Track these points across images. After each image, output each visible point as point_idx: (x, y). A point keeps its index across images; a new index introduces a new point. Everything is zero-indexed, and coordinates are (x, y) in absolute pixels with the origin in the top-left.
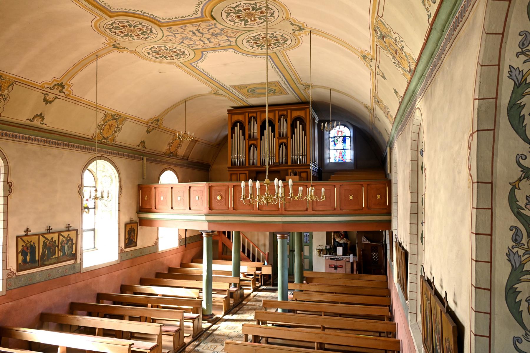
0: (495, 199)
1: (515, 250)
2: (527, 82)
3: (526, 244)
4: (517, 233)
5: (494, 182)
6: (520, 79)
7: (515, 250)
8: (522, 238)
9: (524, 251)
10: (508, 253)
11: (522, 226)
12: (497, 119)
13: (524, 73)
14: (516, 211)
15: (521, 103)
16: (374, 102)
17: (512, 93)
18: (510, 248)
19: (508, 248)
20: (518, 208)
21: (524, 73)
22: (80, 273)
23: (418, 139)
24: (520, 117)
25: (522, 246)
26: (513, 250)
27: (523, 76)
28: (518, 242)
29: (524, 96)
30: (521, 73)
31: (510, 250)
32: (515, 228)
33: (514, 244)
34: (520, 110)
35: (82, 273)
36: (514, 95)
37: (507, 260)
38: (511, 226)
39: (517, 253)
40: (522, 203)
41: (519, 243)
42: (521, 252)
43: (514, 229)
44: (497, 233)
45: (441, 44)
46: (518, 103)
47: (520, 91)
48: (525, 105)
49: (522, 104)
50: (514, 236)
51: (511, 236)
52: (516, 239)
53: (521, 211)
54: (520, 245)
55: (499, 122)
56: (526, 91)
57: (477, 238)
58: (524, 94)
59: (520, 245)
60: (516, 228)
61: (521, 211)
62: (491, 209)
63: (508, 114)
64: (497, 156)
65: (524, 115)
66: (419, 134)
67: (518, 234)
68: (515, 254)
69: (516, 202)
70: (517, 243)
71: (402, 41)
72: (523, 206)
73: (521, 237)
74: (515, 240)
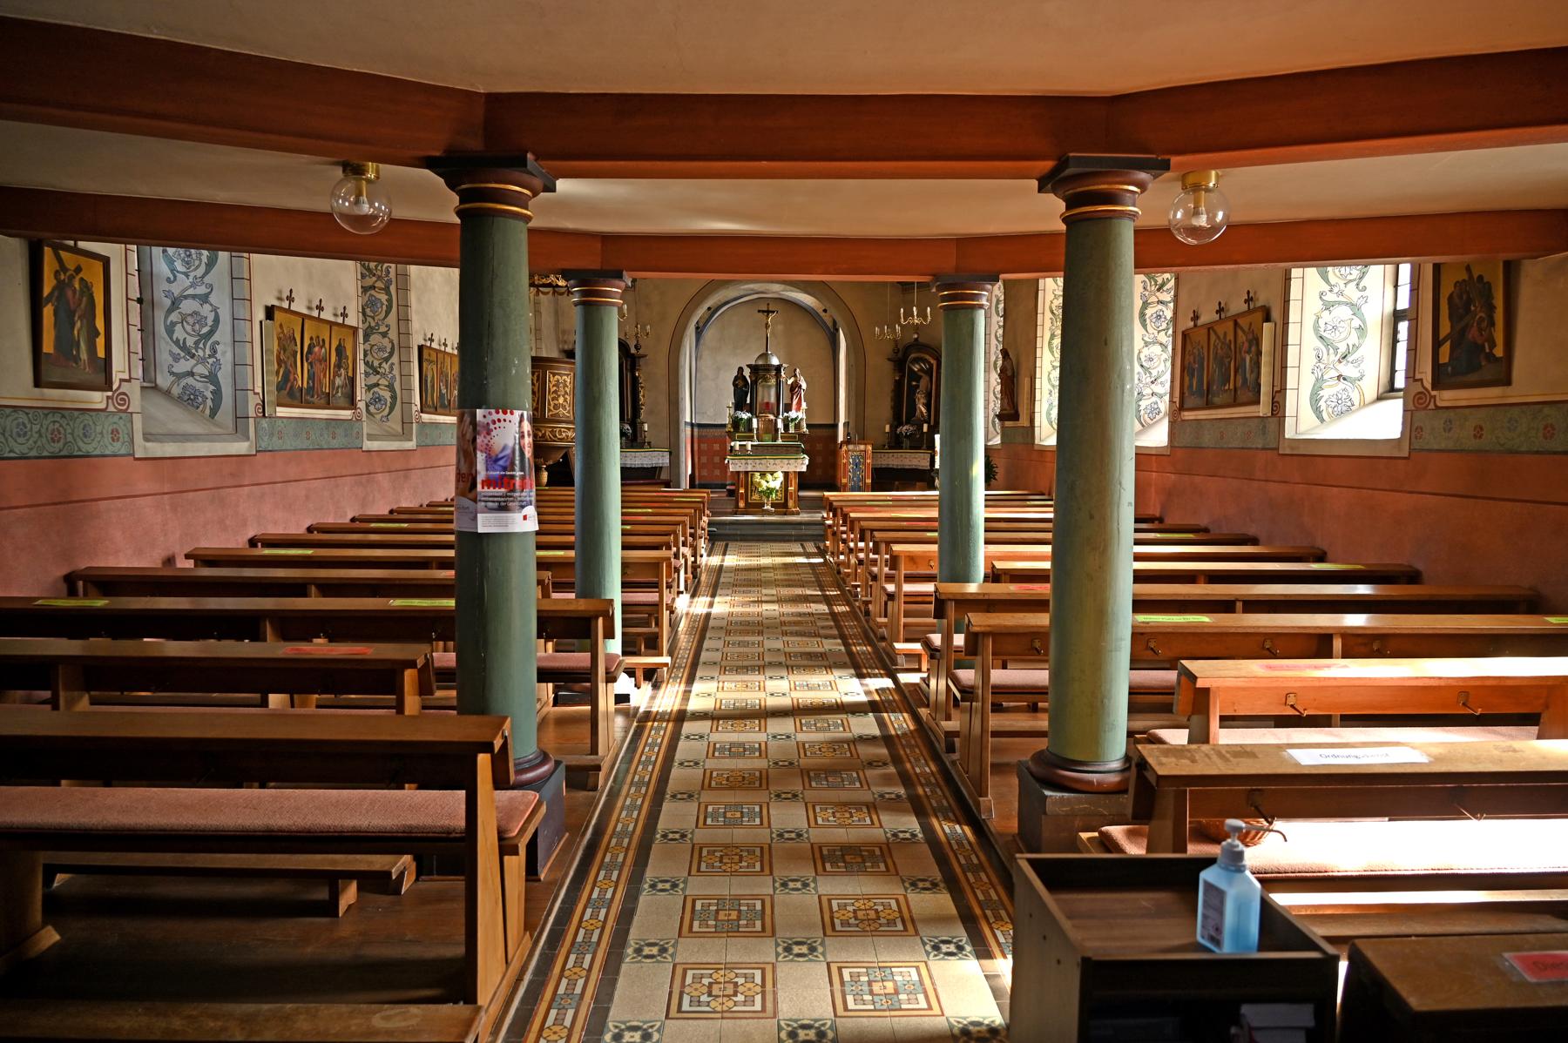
22: (1275, 452)
35: (1283, 455)
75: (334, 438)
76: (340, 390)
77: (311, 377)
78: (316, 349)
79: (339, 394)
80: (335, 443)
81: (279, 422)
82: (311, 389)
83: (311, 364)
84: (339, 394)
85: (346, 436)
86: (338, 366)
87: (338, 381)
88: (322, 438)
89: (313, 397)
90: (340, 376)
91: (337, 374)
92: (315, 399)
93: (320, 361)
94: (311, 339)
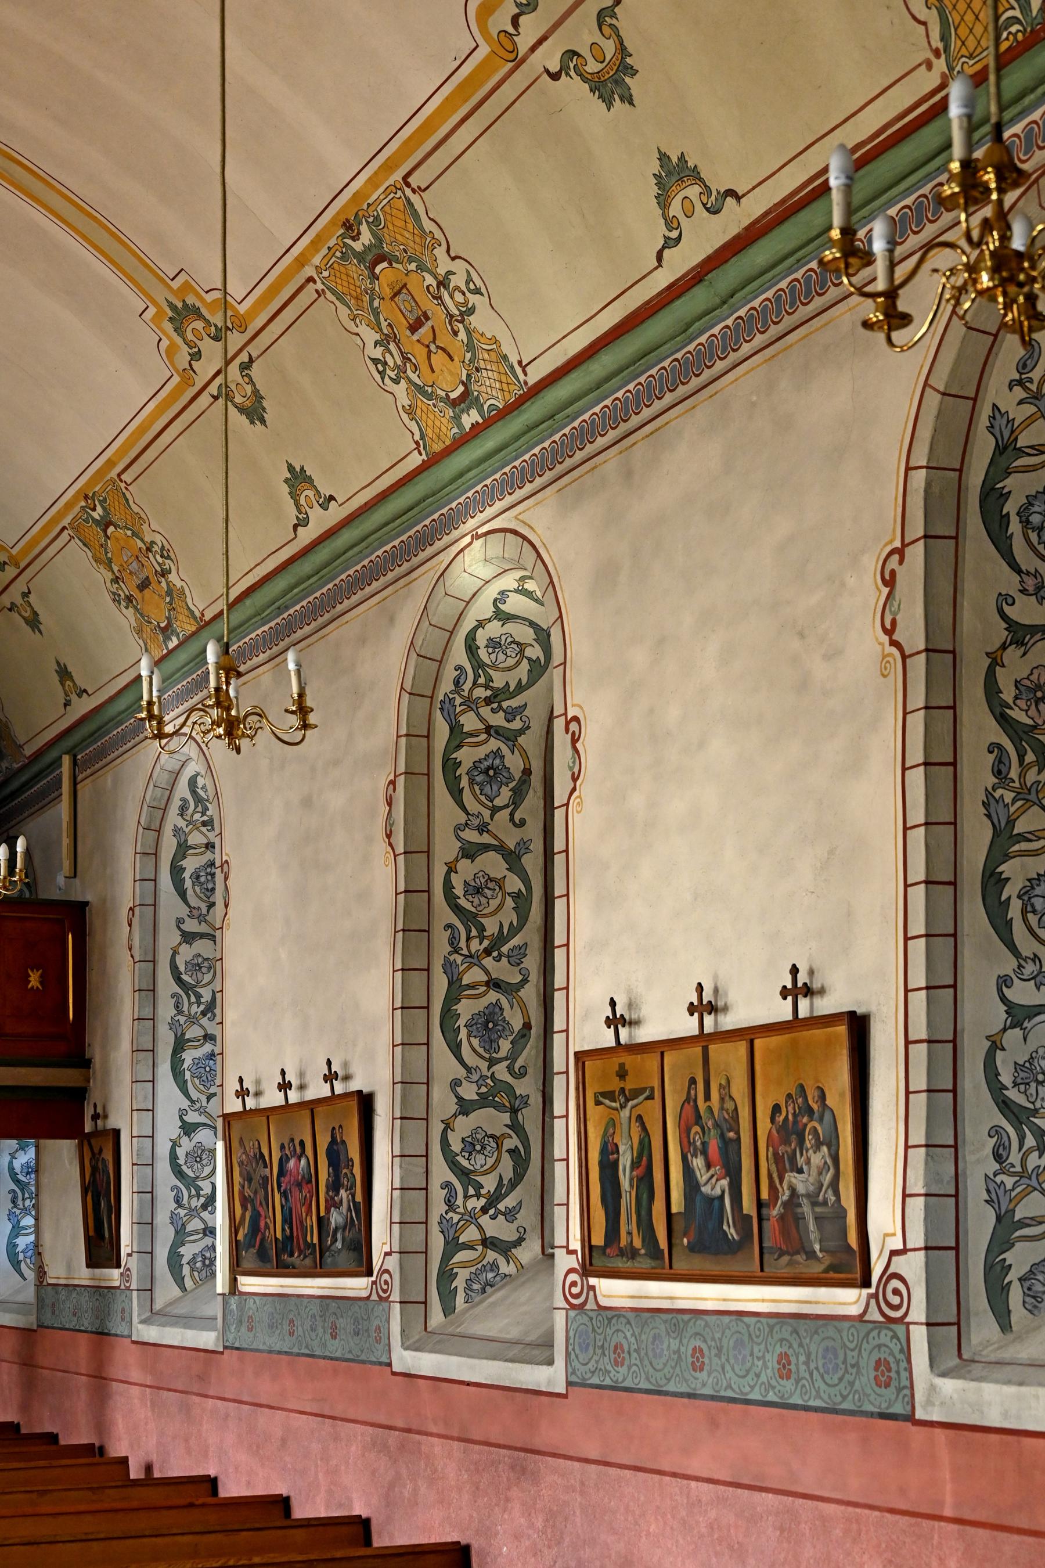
0: (961, 687)
1: (997, 794)
2: (1018, 446)
3: (1016, 778)
4: (1000, 758)
5: (957, 650)
6: (1006, 437)
7: (997, 794)
8: (1010, 768)
9: (1014, 794)
10: (986, 801)
11: (1010, 743)
12: (961, 516)
13: (1015, 426)
14: (998, 710)
15: (1003, 488)
16: (65, 522)
17: (990, 463)
18: (990, 789)
19: (986, 789)
20: (1001, 706)
21: (1015, 426)
23: (444, 653)
24: (1002, 517)
25: (1011, 784)
26: (995, 794)
27: (1012, 432)
28: (1003, 776)
29: (1010, 473)
30: (1010, 425)
31: (989, 796)
32: (998, 748)
33: (997, 781)
34: (1002, 502)
36: (992, 469)
37: (985, 815)
38: (990, 744)
39: (1001, 800)
40: (1009, 695)
41: (1005, 778)
42: (1009, 797)
43: (996, 749)
44: (965, 759)
45: (701, 333)
46: (998, 486)
47: (1003, 461)
48: (1010, 492)
49: (1005, 491)
50: (996, 763)
51: (991, 765)
52: (999, 772)
53: (1008, 711)
54: (1007, 783)
55: (966, 523)
56: (1014, 465)
57: (928, 773)
58: (1009, 471)
59: (1007, 783)
60: (999, 746)
61: (1008, 711)
62: (954, 708)
63: (981, 507)
64: (963, 595)
65: (1008, 514)
66: (452, 633)
67: (1003, 760)
68: (997, 802)
69: (997, 693)
70: (1001, 779)
71: (477, 291)
72: (1010, 702)
73: (1007, 764)
74: (998, 773)
75: (334, 1337)
76: (339, 1236)
77: (287, 1220)
78: (292, 1163)
79: (339, 1245)
80: (336, 1348)
81: (250, 1302)
82: (289, 1239)
83: (284, 1195)
84: (339, 1245)
85: (357, 1334)
86: (335, 1186)
87: (336, 1218)
88: (313, 1335)
89: (291, 1255)
90: (338, 1205)
91: (333, 1203)
92: (295, 1259)
93: (299, 1185)
94: (282, 1147)
